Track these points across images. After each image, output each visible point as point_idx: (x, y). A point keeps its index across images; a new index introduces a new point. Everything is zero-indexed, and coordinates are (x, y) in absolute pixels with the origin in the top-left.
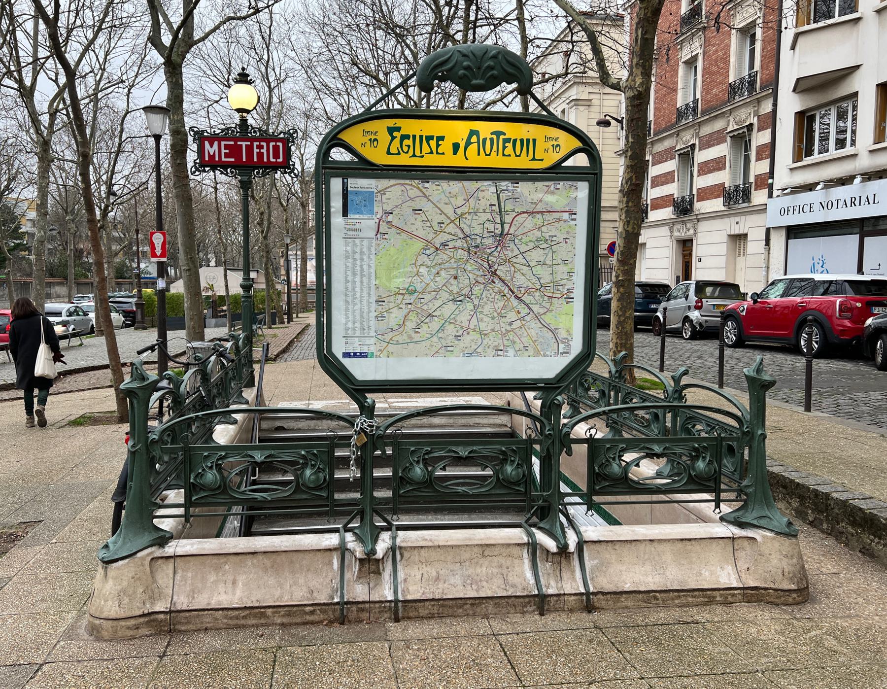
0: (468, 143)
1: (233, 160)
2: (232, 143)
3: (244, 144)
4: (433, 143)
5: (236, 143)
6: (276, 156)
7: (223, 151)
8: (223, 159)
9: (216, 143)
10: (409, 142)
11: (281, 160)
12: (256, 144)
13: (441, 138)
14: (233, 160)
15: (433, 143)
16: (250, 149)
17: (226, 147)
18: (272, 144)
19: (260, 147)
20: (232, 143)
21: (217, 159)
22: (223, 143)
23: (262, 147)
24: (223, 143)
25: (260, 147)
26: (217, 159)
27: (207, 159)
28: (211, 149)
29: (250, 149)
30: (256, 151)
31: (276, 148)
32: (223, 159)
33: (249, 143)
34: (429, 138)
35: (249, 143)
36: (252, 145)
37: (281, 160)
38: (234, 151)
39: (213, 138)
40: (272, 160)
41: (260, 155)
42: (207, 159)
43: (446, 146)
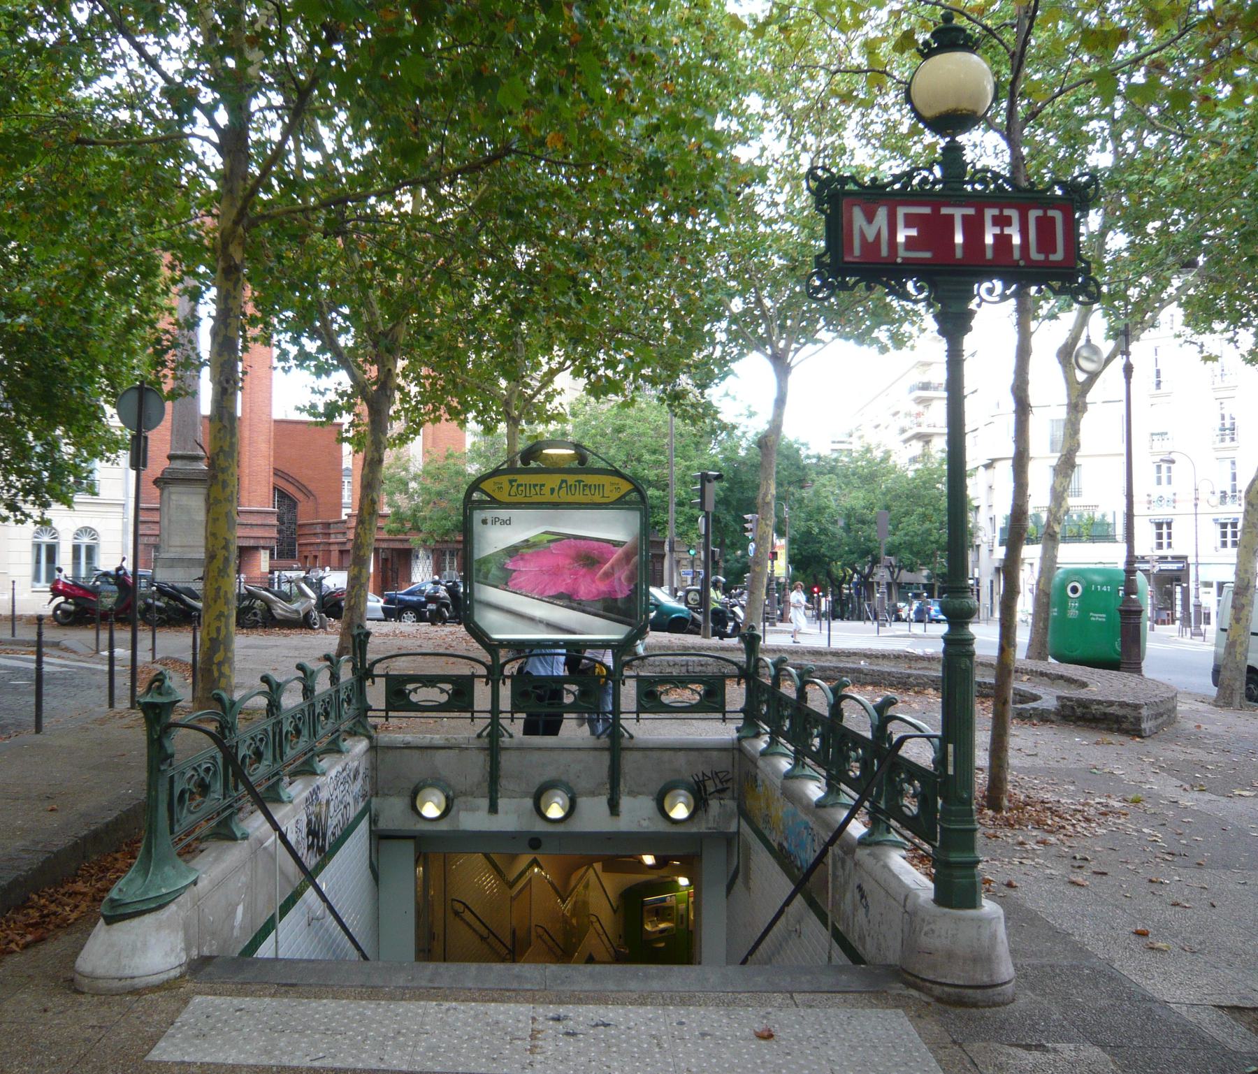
1: (928, 255)
2: (927, 210)
3: (958, 213)
5: (936, 210)
6: (1046, 242)
8: (902, 253)
9: (882, 214)
11: (1058, 256)
14: (928, 255)
17: (910, 221)
18: (1033, 214)
20: (927, 210)
21: (884, 252)
22: (901, 212)
24: (901, 212)
26: (884, 252)
27: (857, 252)
28: (866, 227)
31: (1045, 226)
33: (970, 211)
35: (970, 211)
37: (1058, 256)
38: (934, 231)
39: (875, 194)
40: (1035, 255)
42: (857, 252)
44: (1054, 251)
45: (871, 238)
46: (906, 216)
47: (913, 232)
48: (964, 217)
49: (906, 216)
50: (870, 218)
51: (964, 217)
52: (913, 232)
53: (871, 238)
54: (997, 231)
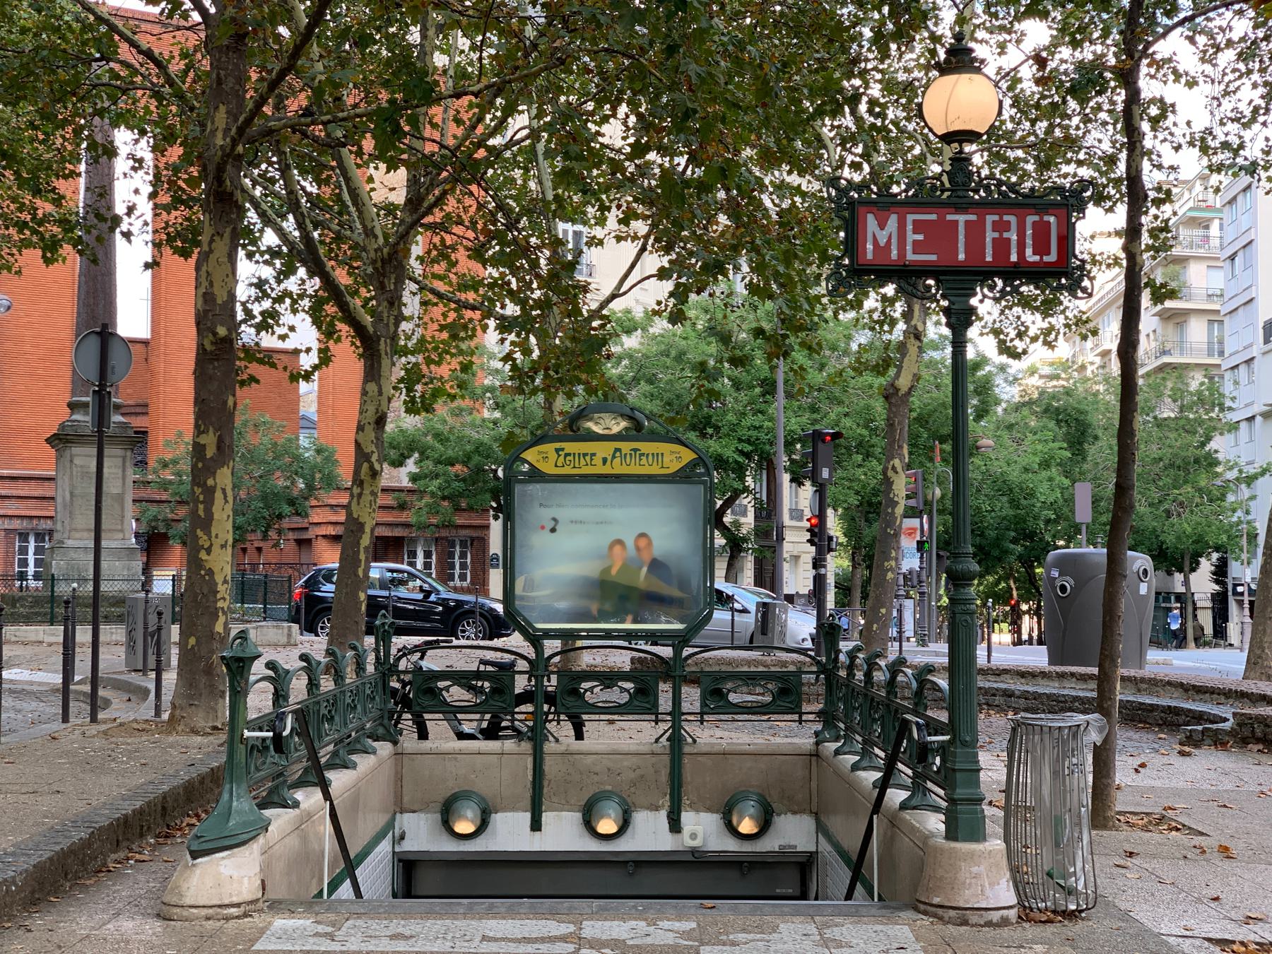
0: (614, 457)
1: (934, 258)
3: (962, 219)
4: (588, 458)
6: (1042, 248)
7: (911, 237)
10: (571, 458)
11: (1052, 257)
12: (990, 219)
13: (594, 455)
15: (588, 458)
16: (975, 231)
17: (918, 227)
18: (1031, 219)
19: (1001, 227)
20: (934, 217)
21: (894, 254)
22: (910, 218)
23: (1005, 227)
24: (910, 218)
25: (1001, 227)
26: (894, 254)
29: (975, 231)
30: (990, 235)
32: (911, 256)
33: (973, 217)
34: (585, 455)
35: (973, 217)
36: (981, 223)
37: (1052, 257)
38: (939, 235)
41: (1002, 246)
42: (870, 256)
43: (598, 461)
44: (1048, 253)
45: (882, 242)
46: (915, 222)
47: (920, 237)
48: (967, 222)
49: (915, 222)
50: (882, 226)
51: (967, 222)
52: (920, 237)
53: (882, 242)
54: (996, 235)
